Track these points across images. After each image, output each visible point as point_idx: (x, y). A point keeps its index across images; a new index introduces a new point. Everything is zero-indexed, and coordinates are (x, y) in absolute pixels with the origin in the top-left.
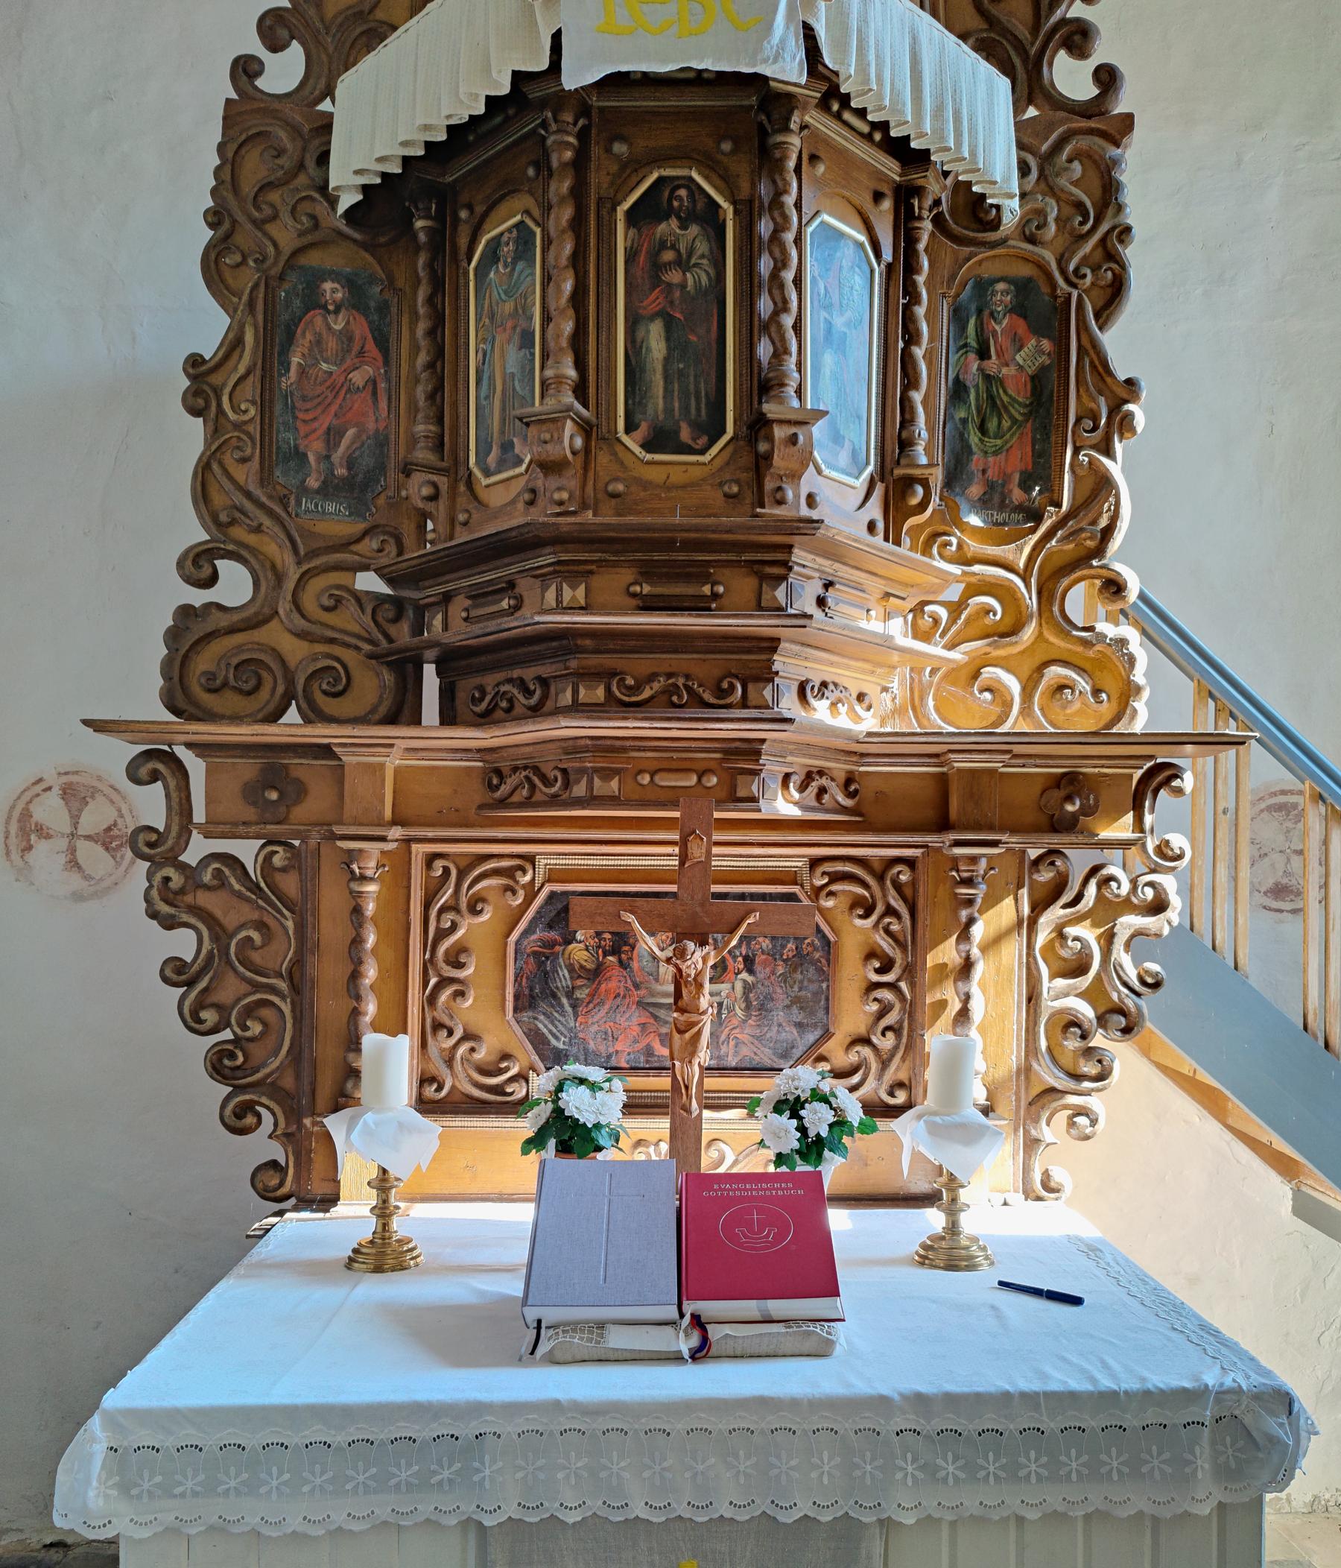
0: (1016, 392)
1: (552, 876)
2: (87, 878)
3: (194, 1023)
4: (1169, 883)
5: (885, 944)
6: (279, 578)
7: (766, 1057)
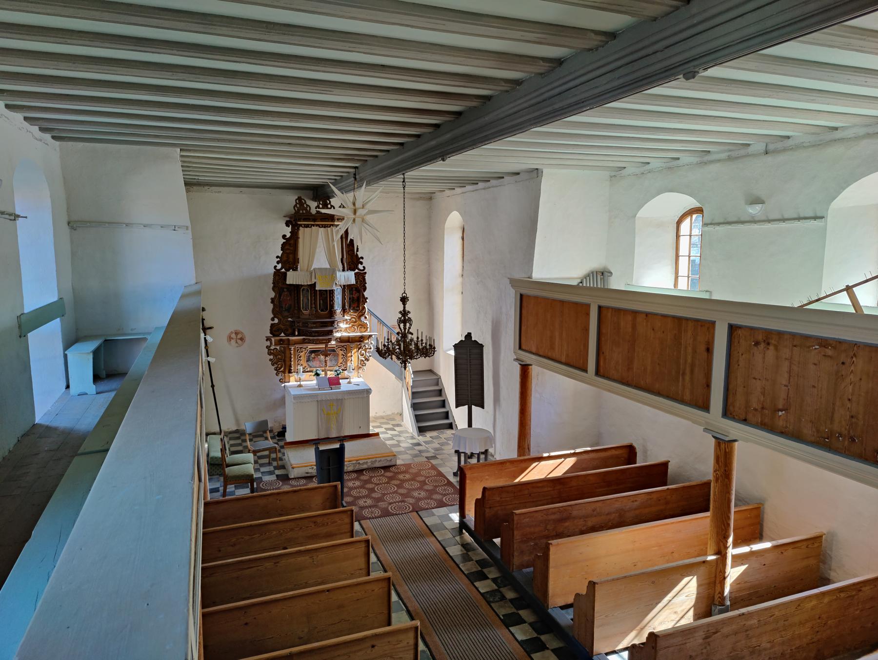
0: (356, 298)
1: (310, 348)
2: (239, 344)
3: (273, 365)
4: (372, 346)
5: (344, 354)
6: (281, 320)
7: (332, 365)
